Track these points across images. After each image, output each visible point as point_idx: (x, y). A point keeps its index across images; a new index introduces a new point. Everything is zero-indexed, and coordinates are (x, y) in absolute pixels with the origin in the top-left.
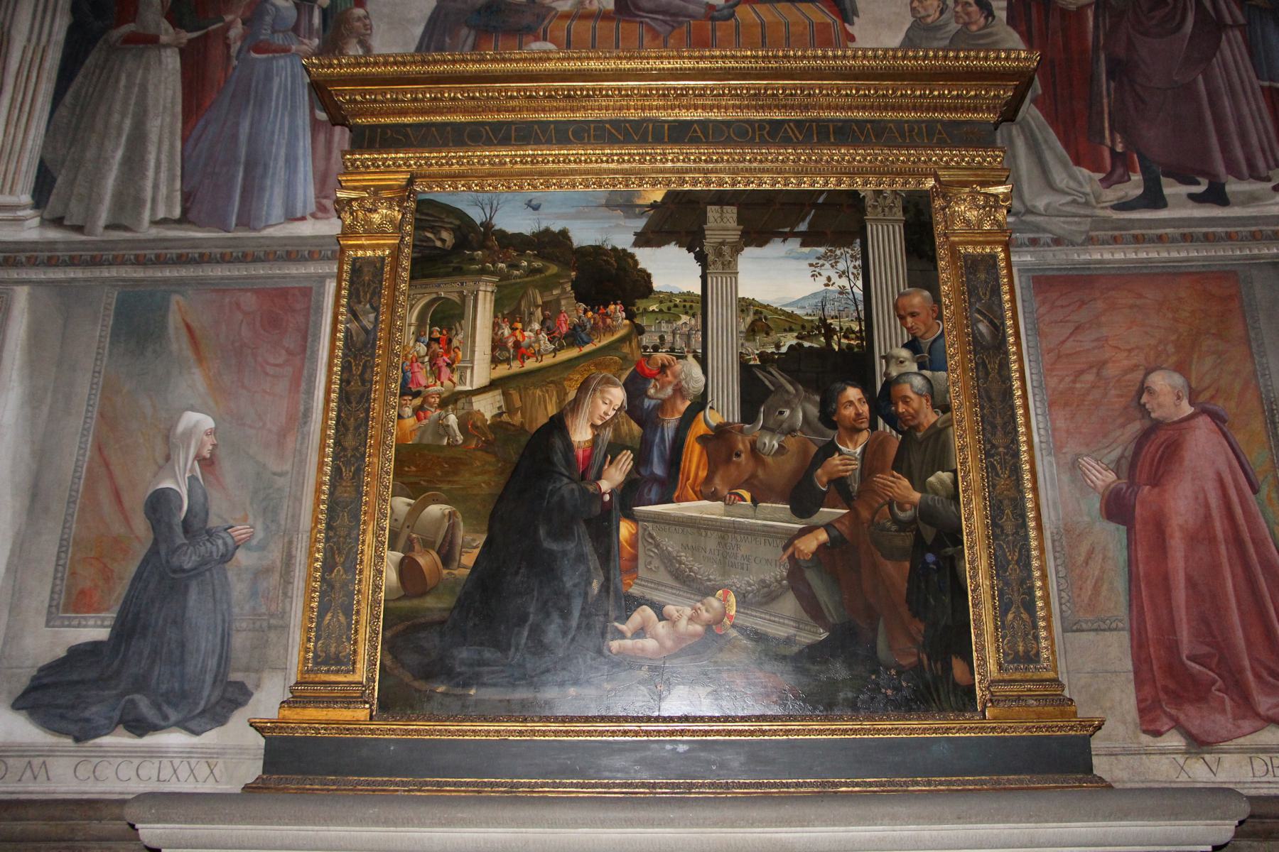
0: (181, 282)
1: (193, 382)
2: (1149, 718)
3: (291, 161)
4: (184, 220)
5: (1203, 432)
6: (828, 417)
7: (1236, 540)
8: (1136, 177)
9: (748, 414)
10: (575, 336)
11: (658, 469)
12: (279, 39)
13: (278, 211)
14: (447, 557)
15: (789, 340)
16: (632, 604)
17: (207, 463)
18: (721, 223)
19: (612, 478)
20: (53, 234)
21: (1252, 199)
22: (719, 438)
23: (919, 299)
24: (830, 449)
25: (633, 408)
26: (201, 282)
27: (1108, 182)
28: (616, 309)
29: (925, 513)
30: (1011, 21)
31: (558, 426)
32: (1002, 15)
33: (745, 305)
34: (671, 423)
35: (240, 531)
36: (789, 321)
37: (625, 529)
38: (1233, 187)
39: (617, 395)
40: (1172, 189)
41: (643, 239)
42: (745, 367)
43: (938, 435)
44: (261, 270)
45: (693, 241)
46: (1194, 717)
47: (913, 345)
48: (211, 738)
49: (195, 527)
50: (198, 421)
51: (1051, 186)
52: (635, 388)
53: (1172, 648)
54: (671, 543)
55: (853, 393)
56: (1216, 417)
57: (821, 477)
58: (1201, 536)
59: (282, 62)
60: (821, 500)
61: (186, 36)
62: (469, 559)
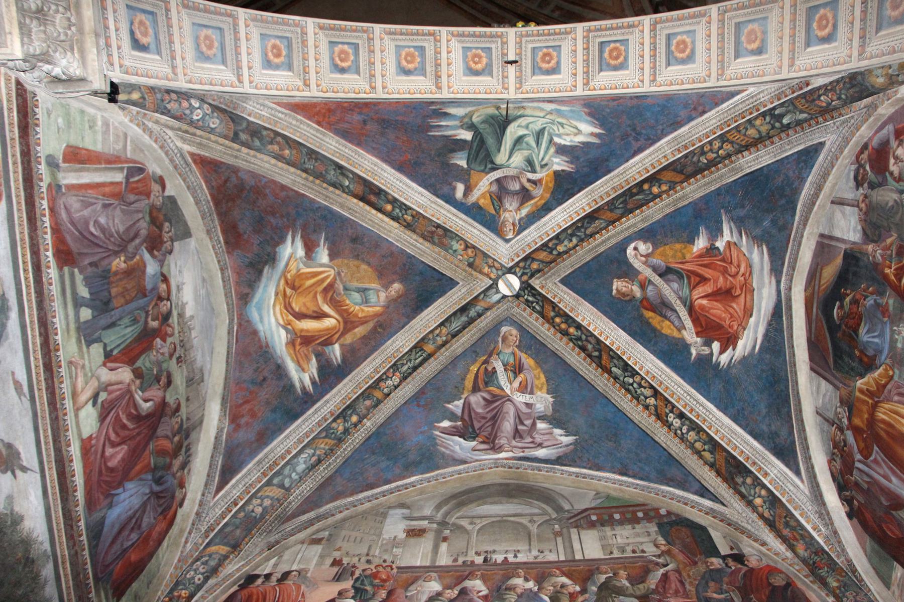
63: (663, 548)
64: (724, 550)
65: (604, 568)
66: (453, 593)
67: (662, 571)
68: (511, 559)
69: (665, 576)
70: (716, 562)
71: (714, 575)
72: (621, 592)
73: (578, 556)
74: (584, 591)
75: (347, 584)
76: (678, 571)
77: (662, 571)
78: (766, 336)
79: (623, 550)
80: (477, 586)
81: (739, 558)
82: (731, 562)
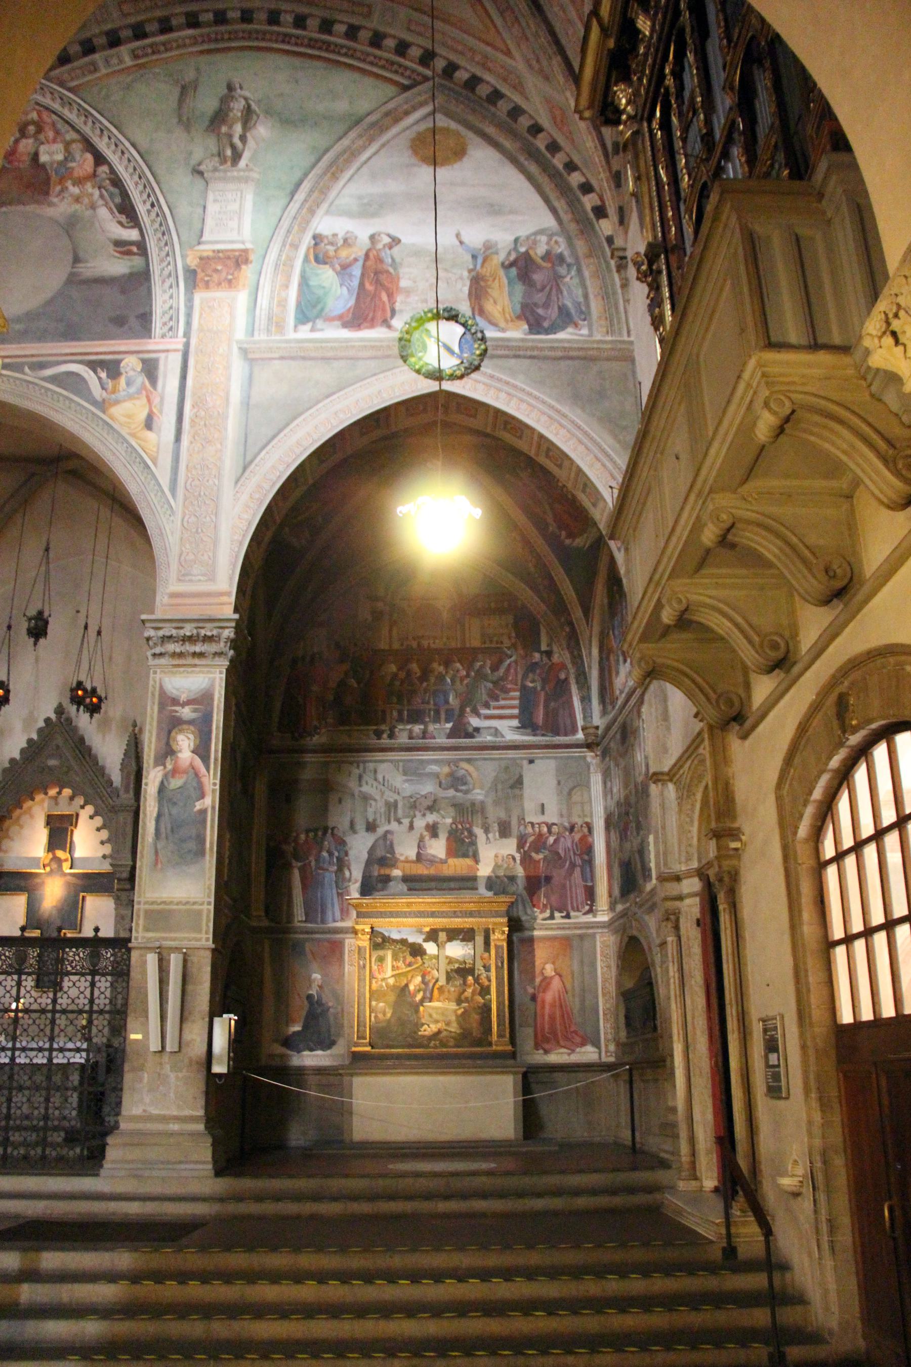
0: (307, 940)
1: (314, 966)
2: (537, 1046)
3: (333, 905)
4: (305, 921)
5: (557, 978)
6: (465, 983)
7: (561, 1006)
8: (548, 911)
9: (448, 982)
10: (410, 965)
11: (428, 995)
12: (325, 866)
13: (330, 919)
14: (384, 1014)
15: (457, 966)
16: (423, 1024)
17: (320, 987)
18: (442, 936)
19: (419, 997)
20: (273, 925)
21: (577, 917)
22: (441, 989)
23: (486, 955)
24: (464, 991)
25: (423, 982)
26: (313, 939)
27: (541, 912)
28: (419, 958)
29: (484, 1005)
30: (522, 863)
31: (407, 985)
32: (518, 862)
33: (447, 957)
34: (431, 985)
35: (330, 1004)
36: (457, 961)
37: (421, 1008)
38: (572, 914)
39: (419, 979)
40: (557, 914)
41: (425, 940)
42: (447, 973)
43: (489, 987)
44: (328, 936)
45: (435, 941)
46: (547, 1046)
47: (484, 967)
48: (329, 1052)
49: (319, 1003)
50: (317, 976)
51: (526, 913)
52: (423, 976)
53: (543, 1029)
54: (431, 1011)
55: (470, 978)
56: (560, 976)
57: (463, 997)
58: (553, 1005)
59: (327, 874)
60: (462, 1002)
61: (299, 864)
62: (389, 1015)
63: (513, 640)
64: (544, 647)
65: (480, 656)
66: (402, 675)
67: (508, 661)
68: (433, 646)
69: (509, 665)
70: (537, 656)
71: (533, 667)
72: (485, 677)
73: (468, 645)
74: (468, 676)
75: (346, 667)
76: (516, 662)
77: (508, 661)
78: (591, 546)
79: (491, 641)
80: (414, 667)
81: (549, 654)
82: (545, 659)
